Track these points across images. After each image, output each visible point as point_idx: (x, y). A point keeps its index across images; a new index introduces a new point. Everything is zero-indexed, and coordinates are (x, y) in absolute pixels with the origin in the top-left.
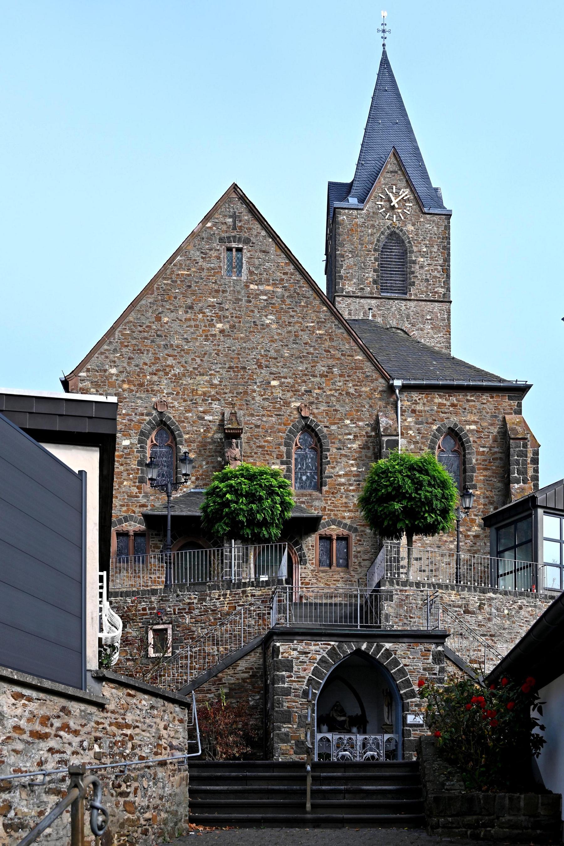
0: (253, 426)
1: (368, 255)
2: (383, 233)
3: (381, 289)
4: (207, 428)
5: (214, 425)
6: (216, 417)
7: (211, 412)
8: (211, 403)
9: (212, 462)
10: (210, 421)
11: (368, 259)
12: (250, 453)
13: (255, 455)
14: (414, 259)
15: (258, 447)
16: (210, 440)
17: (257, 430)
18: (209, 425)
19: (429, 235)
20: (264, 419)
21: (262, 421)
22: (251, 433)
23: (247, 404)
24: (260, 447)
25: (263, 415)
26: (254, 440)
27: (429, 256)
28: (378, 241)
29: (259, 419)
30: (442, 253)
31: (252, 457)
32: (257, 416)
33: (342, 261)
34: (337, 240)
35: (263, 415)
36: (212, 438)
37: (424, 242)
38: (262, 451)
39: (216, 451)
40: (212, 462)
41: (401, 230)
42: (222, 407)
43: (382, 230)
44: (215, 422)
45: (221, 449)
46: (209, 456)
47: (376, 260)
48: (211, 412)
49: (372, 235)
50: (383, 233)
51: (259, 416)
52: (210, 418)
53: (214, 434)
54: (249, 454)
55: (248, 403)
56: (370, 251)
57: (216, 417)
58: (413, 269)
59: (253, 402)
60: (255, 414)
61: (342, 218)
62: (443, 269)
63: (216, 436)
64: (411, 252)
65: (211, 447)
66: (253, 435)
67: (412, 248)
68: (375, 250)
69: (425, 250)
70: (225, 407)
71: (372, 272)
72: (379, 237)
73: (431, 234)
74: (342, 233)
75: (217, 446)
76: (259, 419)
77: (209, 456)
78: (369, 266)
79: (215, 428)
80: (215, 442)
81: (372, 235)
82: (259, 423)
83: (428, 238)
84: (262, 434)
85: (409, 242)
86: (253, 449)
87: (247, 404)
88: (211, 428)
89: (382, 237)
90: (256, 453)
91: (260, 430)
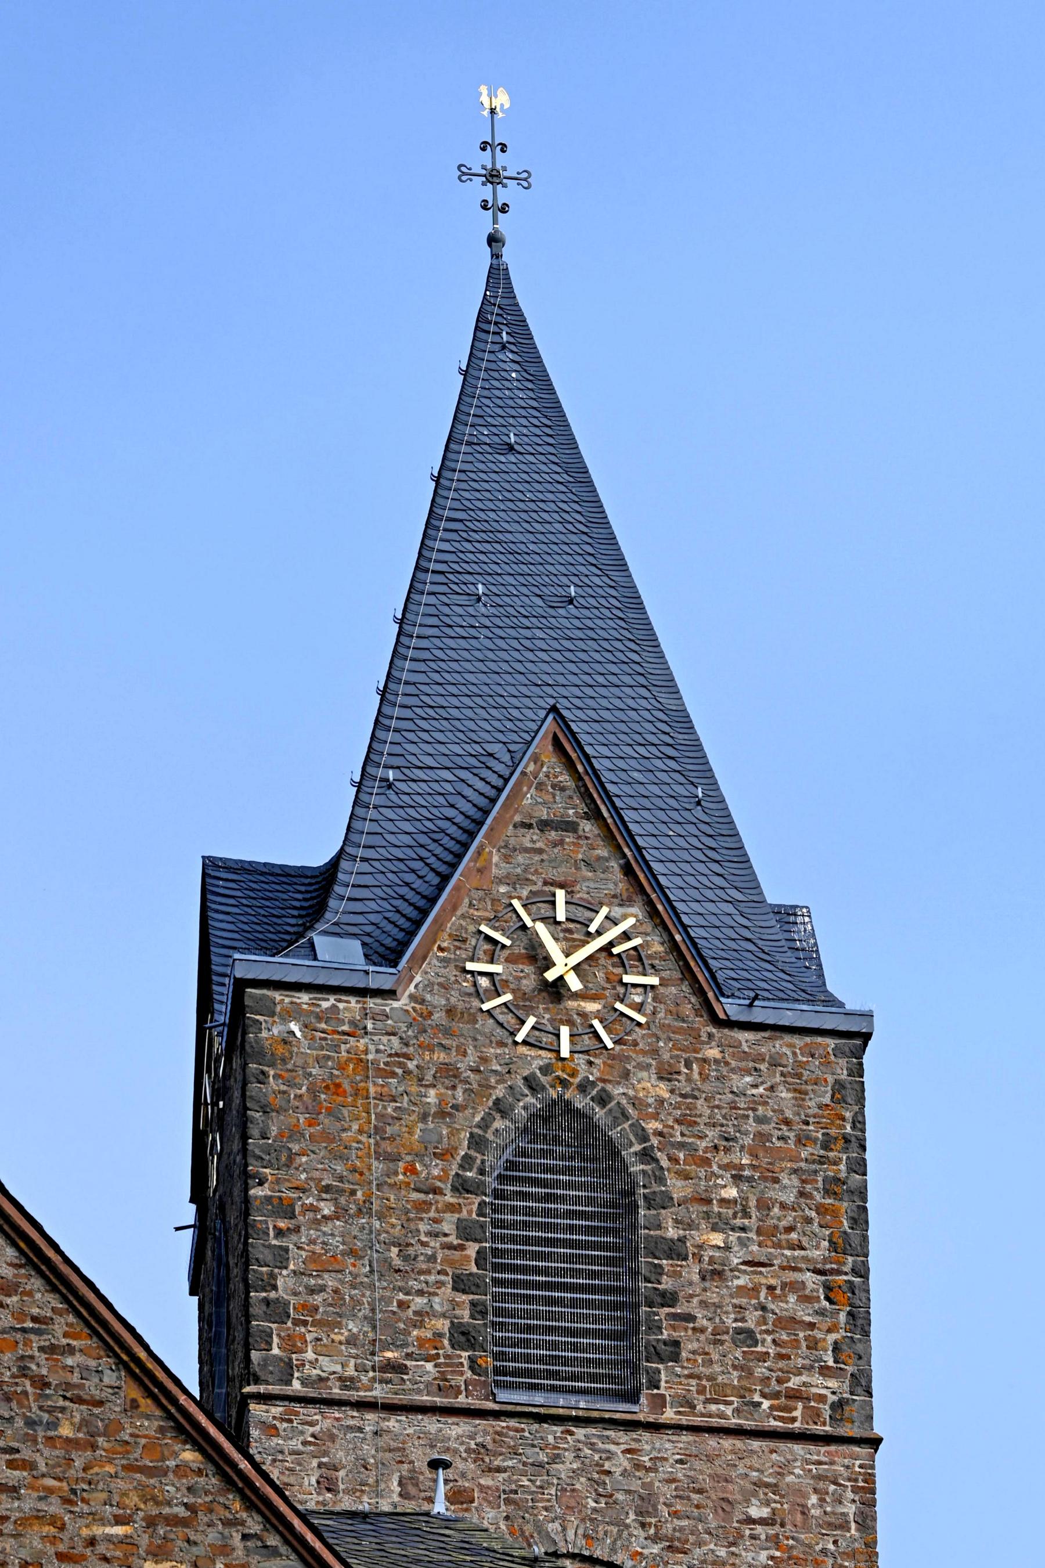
1: (422, 1207)
2: (501, 1108)
3: (497, 1371)
11: (423, 1227)
14: (672, 1233)
19: (751, 1126)
27: (752, 1222)
28: (477, 1142)
30: (821, 1210)
33: (280, 1233)
34: (254, 1131)
37: (723, 1158)
41: (603, 1099)
43: (500, 1092)
47: (466, 1231)
49: (442, 1114)
50: (501, 1108)
56: (436, 1191)
58: (667, 1284)
61: (281, 1026)
62: (828, 1288)
64: (660, 1202)
67: (661, 1180)
68: (462, 1187)
69: (732, 1193)
71: (447, 1290)
72: (485, 1124)
73: (759, 1120)
74: (279, 1102)
78: (432, 1258)
81: (442, 1114)
83: (748, 1141)
85: (646, 1156)
89: (499, 1124)
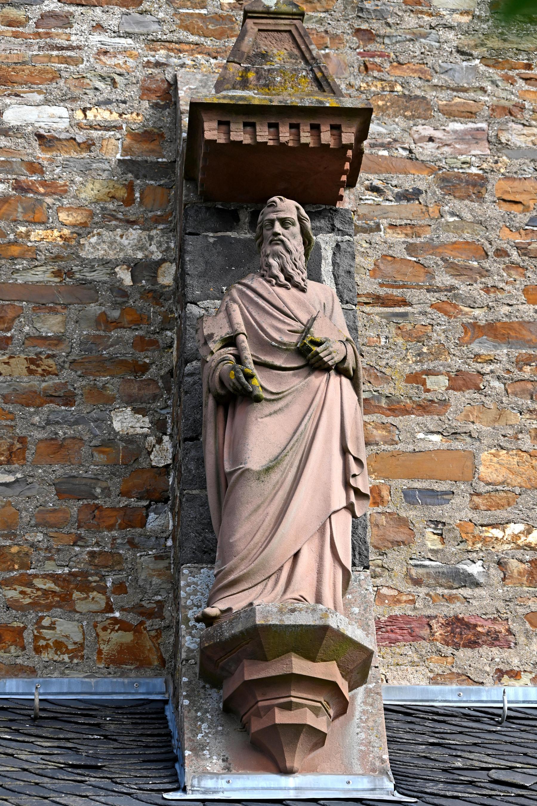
0: (423, 181)
4: (19, 187)
5: (86, 170)
6: (103, 115)
7: (56, 76)
8: (66, 21)
9: (57, 448)
10: (45, 140)
12: (415, 379)
13: (459, 399)
15: (474, 329)
16: (42, 275)
17: (466, 208)
18: (34, 167)
20: (516, 136)
21: (499, 145)
22: (412, 229)
23: (367, 36)
24: (495, 331)
25: (512, 112)
26: (444, 279)
29: (475, 137)
31: (424, 408)
32: (451, 114)
35: (512, 112)
36: (64, 262)
38: (521, 363)
39: (92, 361)
40: (57, 448)
42: (153, 43)
44: (88, 145)
45: (142, 343)
46: (32, 399)
48: (56, 76)
51: (471, 115)
52: (55, 117)
53: (82, 230)
54: (399, 389)
55: (376, 26)
57: (103, 115)
59: (411, 21)
60: (441, 99)
63: (94, 247)
65: (51, 325)
66: (430, 247)
70: (175, 46)
75: (104, 322)
76: (475, 137)
77: (32, 399)
79: (90, 191)
80: (87, 290)
82: (475, 158)
84: (506, 238)
86: (440, 351)
87: (367, 36)
88: (54, 189)
90: (460, 381)
91: (493, 211)
